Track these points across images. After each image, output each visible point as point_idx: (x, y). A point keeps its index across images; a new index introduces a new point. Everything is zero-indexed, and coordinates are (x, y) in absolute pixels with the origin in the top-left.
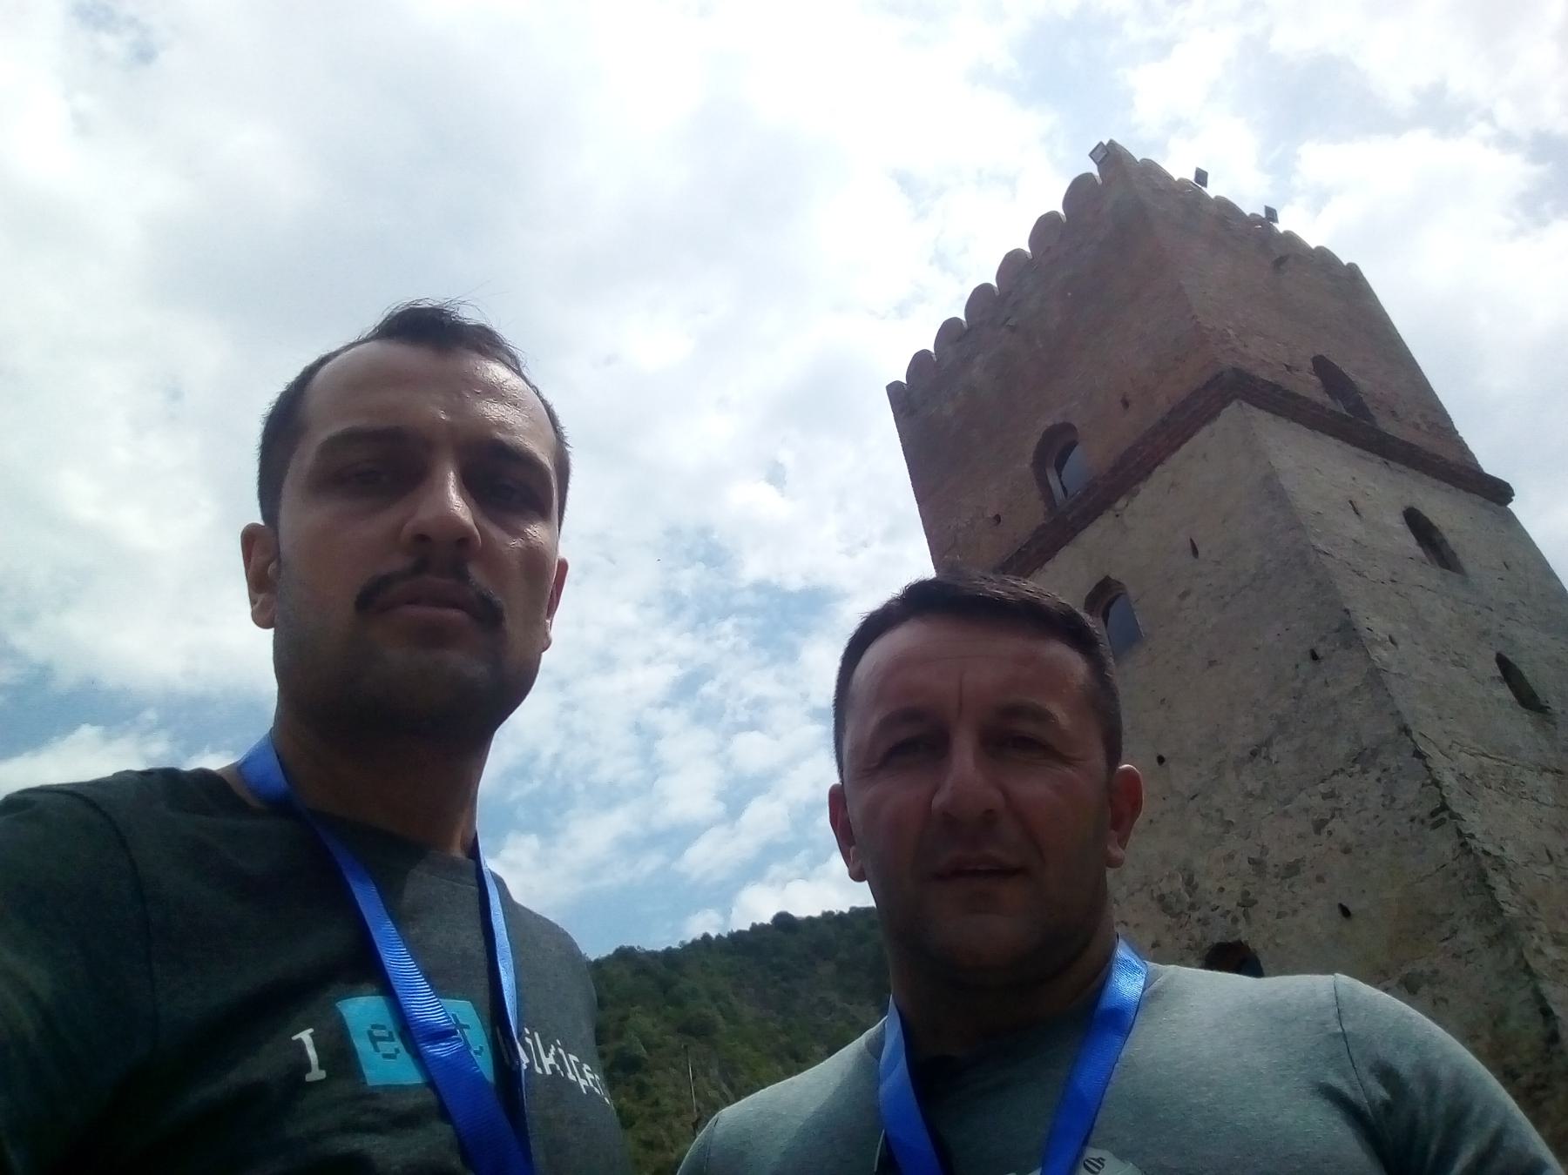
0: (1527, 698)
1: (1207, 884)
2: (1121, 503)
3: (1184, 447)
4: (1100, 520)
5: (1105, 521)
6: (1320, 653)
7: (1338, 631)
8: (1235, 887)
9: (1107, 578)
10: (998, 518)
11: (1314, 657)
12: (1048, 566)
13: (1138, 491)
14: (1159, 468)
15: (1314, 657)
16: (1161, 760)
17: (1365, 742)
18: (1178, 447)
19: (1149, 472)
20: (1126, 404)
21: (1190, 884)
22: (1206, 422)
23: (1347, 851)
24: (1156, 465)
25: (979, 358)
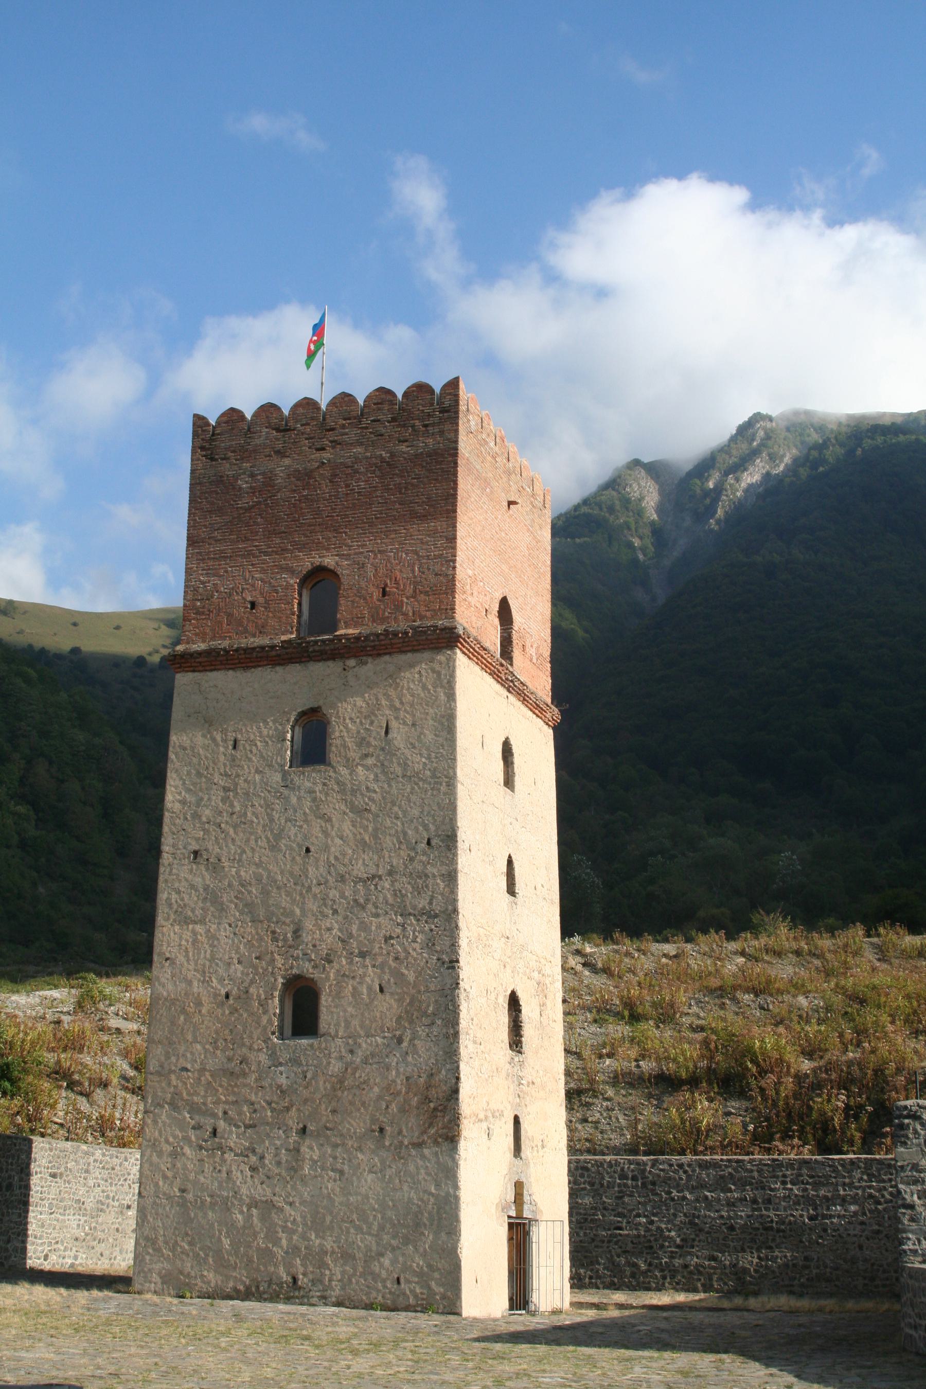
0: (511, 889)
1: (306, 938)
2: (352, 662)
3: (409, 655)
4: (330, 663)
5: (333, 667)
6: (433, 842)
7: (448, 836)
8: (324, 949)
9: (319, 707)
10: (253, 605)
11: (429, 843)
12: (278, 668)
13: (366, 663)
14: (387, 658)
15: (429, 843)
16: (308, 850)
17: (434, 907)
18: (405, 652)
19: (379, 655)
20: (384, 593)
21: (297, 933)
22: (433, 649)
23: (396, 958)
24: (385, 654)
25: (287, 461)
